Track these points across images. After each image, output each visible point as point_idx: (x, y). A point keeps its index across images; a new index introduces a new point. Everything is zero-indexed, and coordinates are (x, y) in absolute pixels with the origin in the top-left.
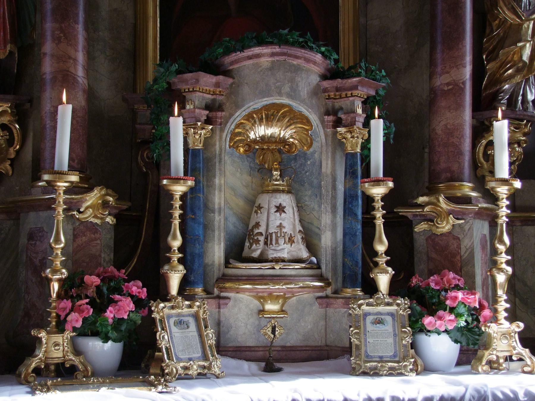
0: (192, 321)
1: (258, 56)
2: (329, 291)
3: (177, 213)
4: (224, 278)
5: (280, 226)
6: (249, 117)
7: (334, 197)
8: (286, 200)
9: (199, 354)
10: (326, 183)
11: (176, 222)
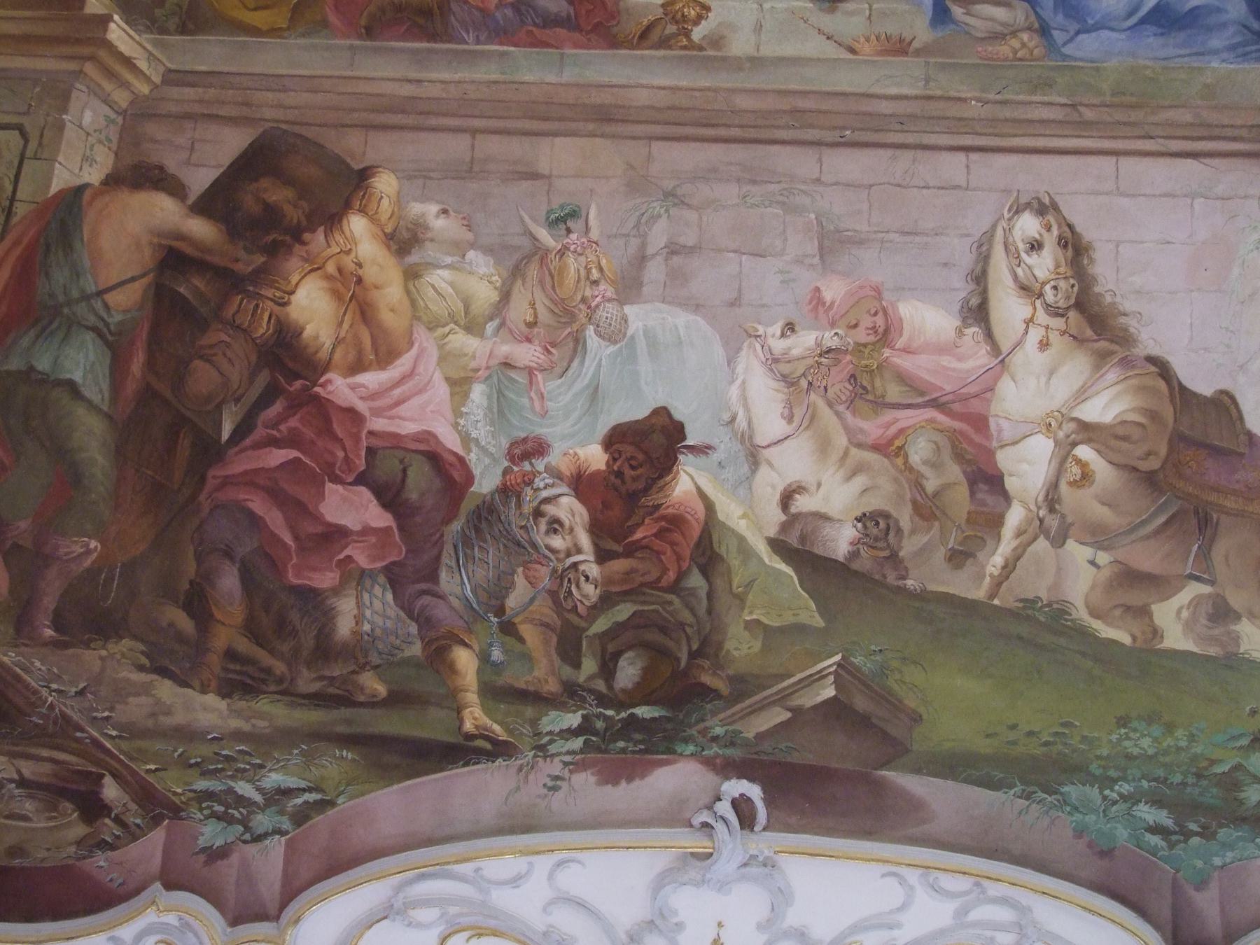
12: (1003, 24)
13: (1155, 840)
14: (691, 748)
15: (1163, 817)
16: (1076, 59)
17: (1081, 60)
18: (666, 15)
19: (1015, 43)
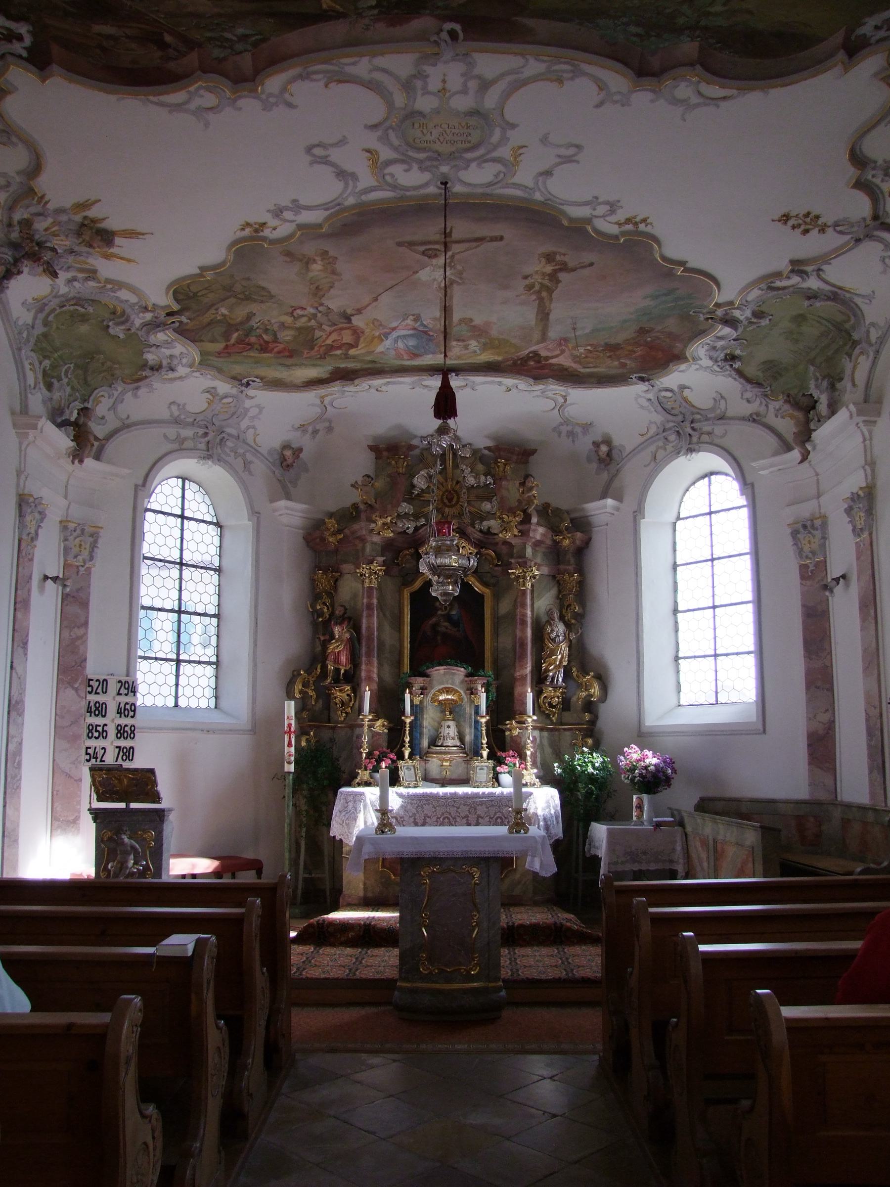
0: (412, 768)
1: (439, 670)
2: (468, 758)
3: (408, 729)
4: (428, 753)
5: (448, 733)
6: (439, 691)
7: (471, 722)
8: (452, 723)
9: (414, 779)
10: (467, 716)
11: (407, 732)
13: (634, 39)
14: (428, 12)
15: (639, 30)
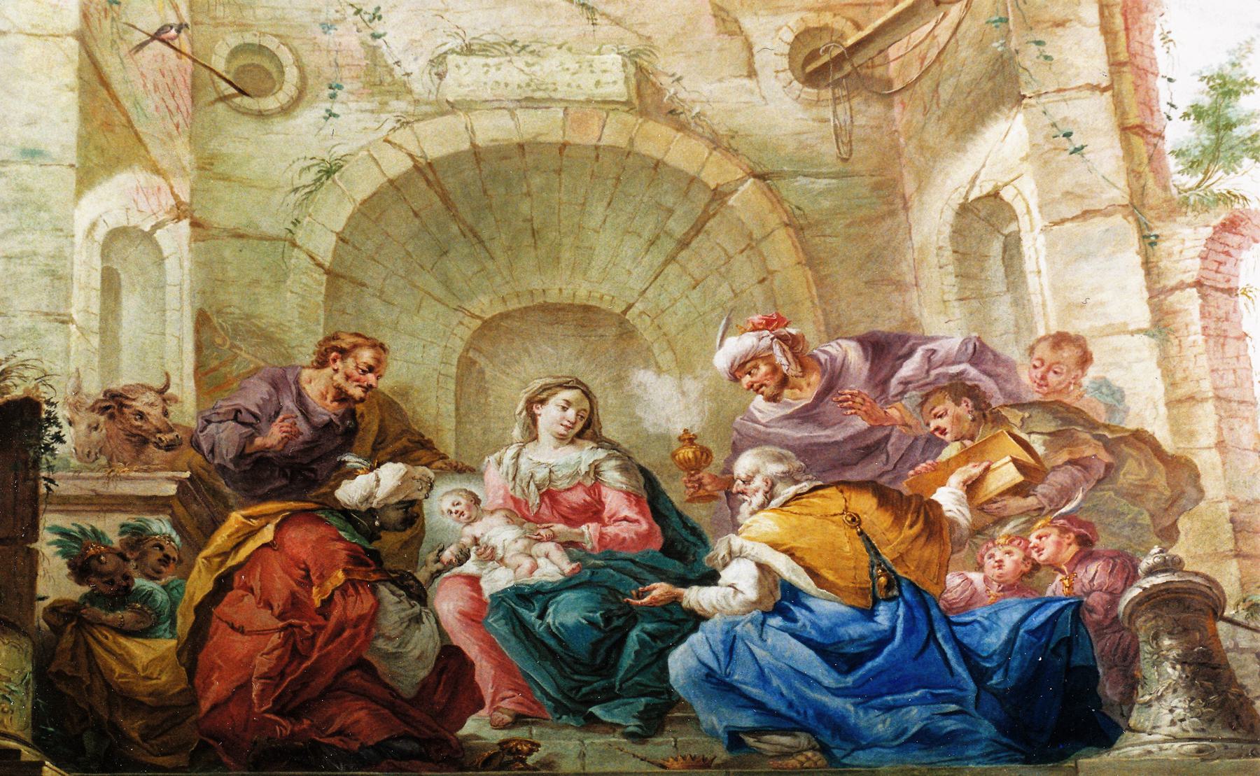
12: (788, 747)
16: (853, 766)
17: (857, 766)
18: (503, 750)
19: (801, 758)
